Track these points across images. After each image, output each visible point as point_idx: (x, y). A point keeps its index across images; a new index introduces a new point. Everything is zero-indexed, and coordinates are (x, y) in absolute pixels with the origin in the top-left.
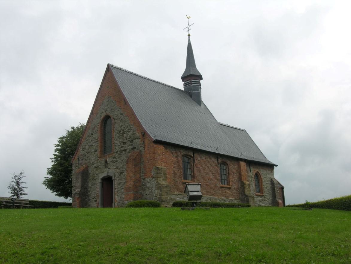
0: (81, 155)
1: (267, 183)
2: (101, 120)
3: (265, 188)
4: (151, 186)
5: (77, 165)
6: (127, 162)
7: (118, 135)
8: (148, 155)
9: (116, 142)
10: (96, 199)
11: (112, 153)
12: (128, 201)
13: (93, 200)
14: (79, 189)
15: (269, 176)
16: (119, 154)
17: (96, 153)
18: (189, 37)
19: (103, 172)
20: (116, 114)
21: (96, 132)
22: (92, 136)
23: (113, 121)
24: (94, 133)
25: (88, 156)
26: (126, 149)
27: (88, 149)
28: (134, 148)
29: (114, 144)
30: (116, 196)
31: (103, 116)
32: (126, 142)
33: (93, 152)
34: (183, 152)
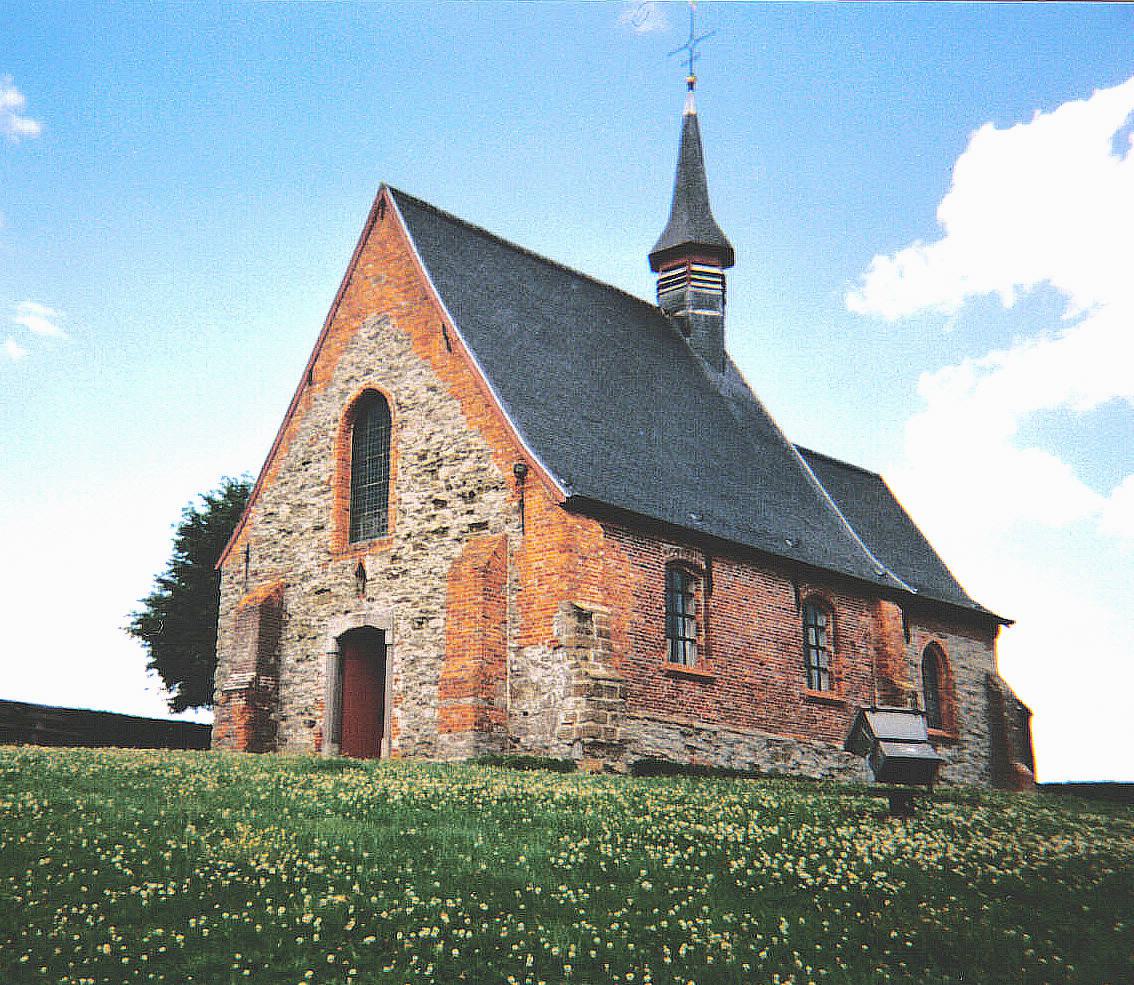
0: (260, 541)
1: (973, 689)
2: (346, 408)
3: (962, 712)
4: (546, 680)
5: (239, 577)
6: (454, 578)
7: (413, 470)
8: (540, 556)
9: (406, 497)
10: (312, 718)
11: (386, 538)
12: (452, 735)
13: (301, 719)
14: (249, 676)
15: (979, 662)
16: (416, 547)
17: (321, 534)
21: (323, 453)
22: (306, 470)
23: (397, 416)
24: (312, 459)
25: (286, 546)
26: (444, 526)
29: (394, 503)
31: (355, 391)
34: (669, 551)
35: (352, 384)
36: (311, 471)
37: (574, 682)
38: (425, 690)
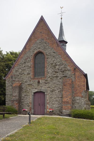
0: (14, 75)
2: (34, 54)
13: (26, 105)
18: (61, 19)
19: (36, 89)
20: (48, 52)
23: (46, 57)
27: (21, 72)
28: (65, 77)
29: (46, 71)
30: (48, 105)
32: (58, 71)
33: (26, 74)
35: (35, 50)
36: (26, 64)
37: (86, 103)
38: (53, 102)
